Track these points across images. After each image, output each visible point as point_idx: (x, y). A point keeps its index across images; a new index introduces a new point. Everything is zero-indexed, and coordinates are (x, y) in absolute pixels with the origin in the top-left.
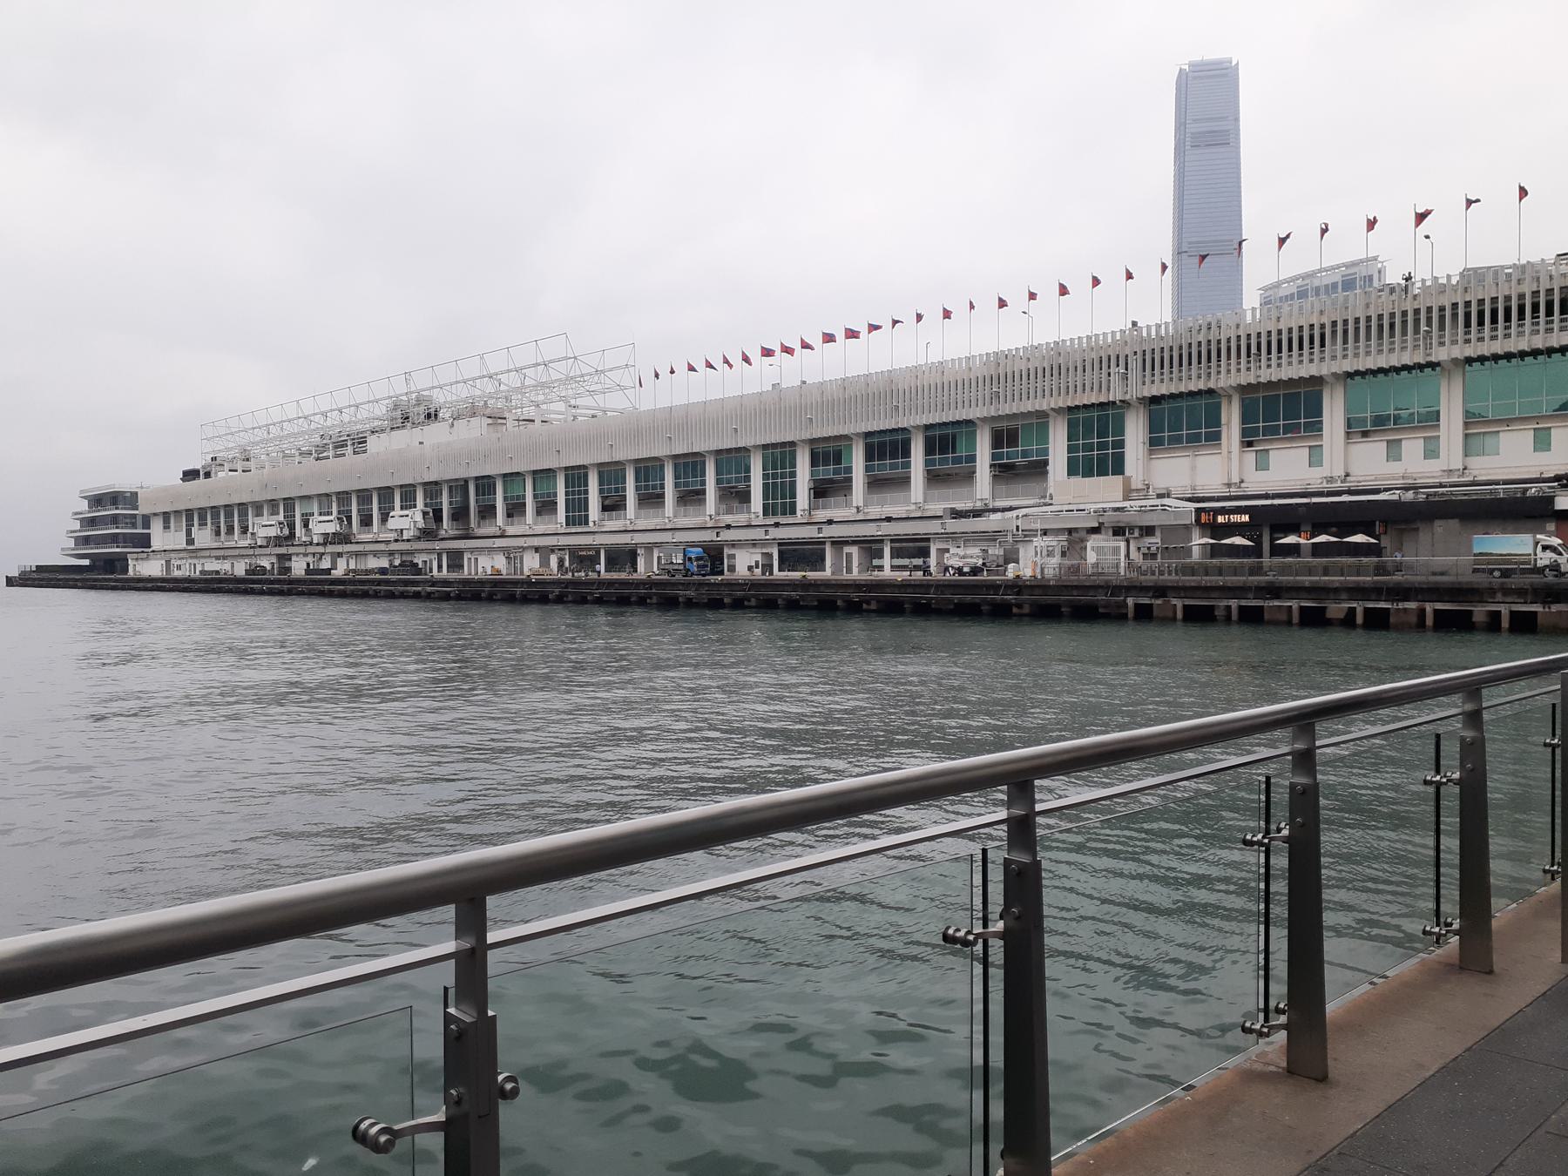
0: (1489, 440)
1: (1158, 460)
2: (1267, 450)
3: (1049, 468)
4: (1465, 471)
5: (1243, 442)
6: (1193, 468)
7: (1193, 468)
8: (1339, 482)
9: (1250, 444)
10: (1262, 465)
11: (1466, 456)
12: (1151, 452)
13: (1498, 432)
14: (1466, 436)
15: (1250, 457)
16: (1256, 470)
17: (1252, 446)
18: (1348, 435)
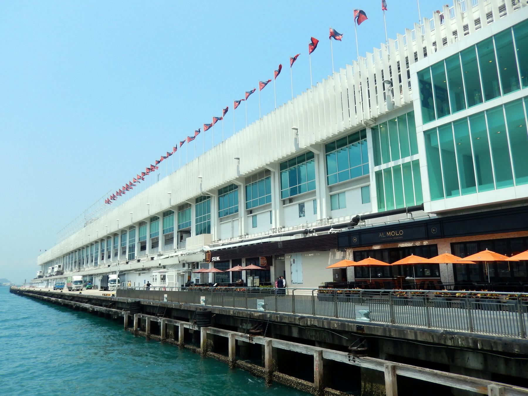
0: (341, 196)
1: (222, 224)
2: (256, 215)
3: (191, 232)
4: (330, 220)
5: (248, 211)
6: (233, 227)
7: (233, 227)
8: (277, 232)
9: (251, 212)
10: (254, 225)
11: (332, 210)
12: (221, 220)
13: (344, 192)
14: (331, 196)
15: (251, 219)
16: (257, 227)
17: (252, 213)
18: (284, 202)
